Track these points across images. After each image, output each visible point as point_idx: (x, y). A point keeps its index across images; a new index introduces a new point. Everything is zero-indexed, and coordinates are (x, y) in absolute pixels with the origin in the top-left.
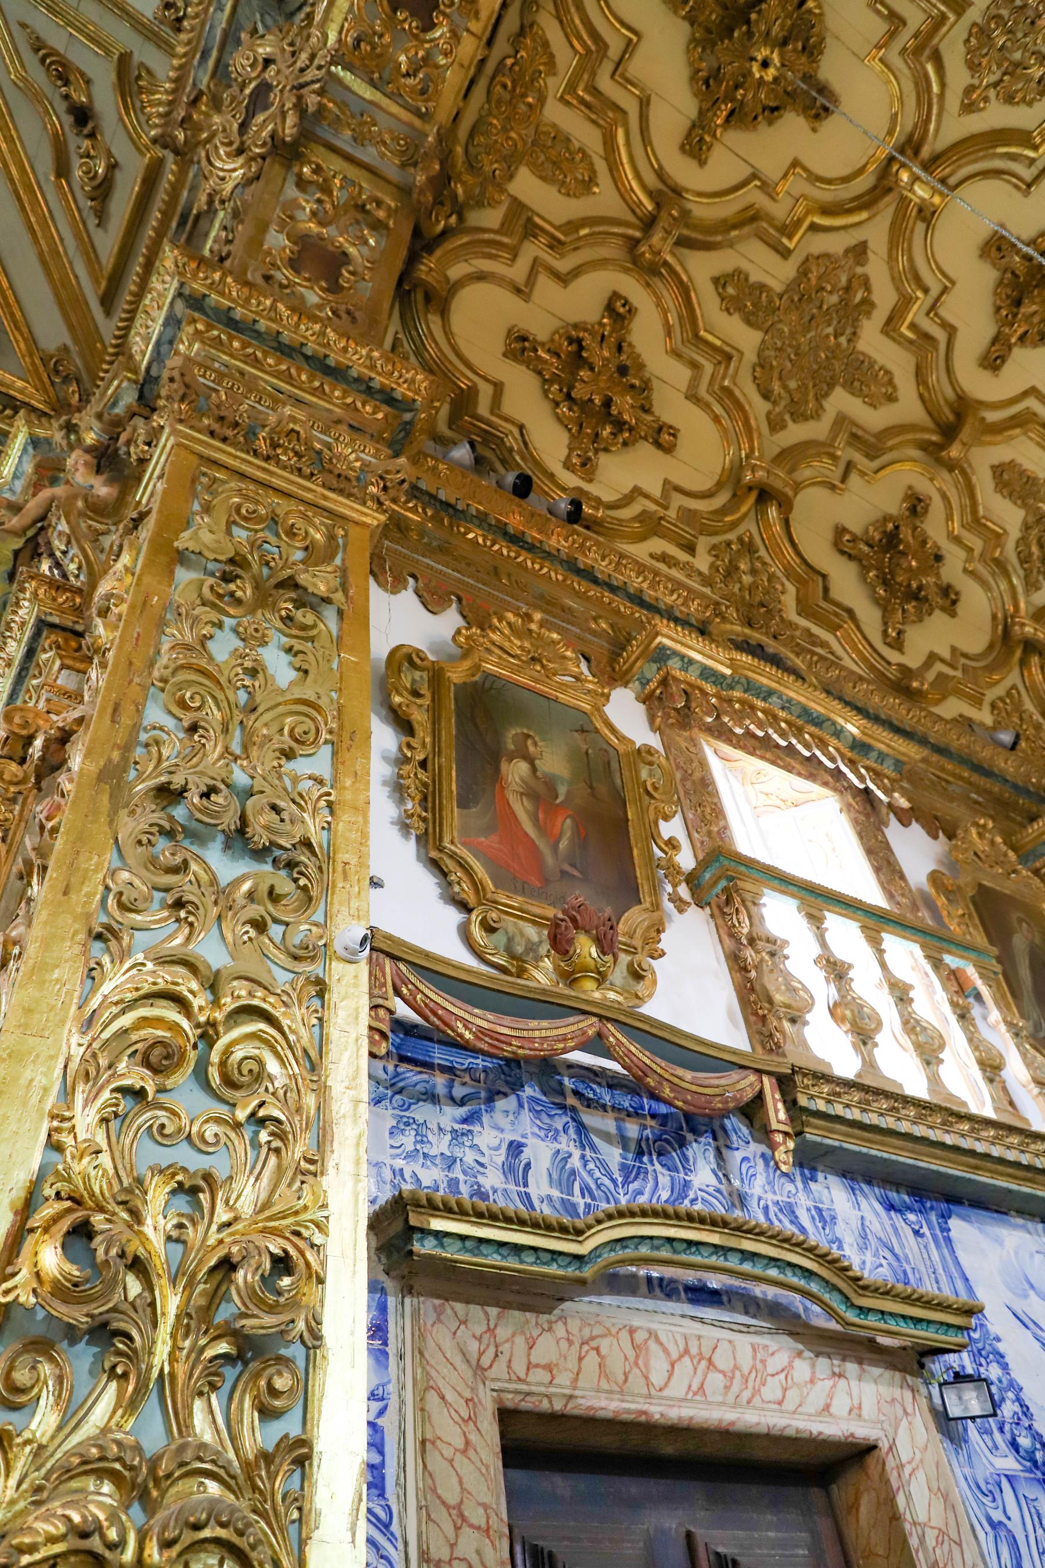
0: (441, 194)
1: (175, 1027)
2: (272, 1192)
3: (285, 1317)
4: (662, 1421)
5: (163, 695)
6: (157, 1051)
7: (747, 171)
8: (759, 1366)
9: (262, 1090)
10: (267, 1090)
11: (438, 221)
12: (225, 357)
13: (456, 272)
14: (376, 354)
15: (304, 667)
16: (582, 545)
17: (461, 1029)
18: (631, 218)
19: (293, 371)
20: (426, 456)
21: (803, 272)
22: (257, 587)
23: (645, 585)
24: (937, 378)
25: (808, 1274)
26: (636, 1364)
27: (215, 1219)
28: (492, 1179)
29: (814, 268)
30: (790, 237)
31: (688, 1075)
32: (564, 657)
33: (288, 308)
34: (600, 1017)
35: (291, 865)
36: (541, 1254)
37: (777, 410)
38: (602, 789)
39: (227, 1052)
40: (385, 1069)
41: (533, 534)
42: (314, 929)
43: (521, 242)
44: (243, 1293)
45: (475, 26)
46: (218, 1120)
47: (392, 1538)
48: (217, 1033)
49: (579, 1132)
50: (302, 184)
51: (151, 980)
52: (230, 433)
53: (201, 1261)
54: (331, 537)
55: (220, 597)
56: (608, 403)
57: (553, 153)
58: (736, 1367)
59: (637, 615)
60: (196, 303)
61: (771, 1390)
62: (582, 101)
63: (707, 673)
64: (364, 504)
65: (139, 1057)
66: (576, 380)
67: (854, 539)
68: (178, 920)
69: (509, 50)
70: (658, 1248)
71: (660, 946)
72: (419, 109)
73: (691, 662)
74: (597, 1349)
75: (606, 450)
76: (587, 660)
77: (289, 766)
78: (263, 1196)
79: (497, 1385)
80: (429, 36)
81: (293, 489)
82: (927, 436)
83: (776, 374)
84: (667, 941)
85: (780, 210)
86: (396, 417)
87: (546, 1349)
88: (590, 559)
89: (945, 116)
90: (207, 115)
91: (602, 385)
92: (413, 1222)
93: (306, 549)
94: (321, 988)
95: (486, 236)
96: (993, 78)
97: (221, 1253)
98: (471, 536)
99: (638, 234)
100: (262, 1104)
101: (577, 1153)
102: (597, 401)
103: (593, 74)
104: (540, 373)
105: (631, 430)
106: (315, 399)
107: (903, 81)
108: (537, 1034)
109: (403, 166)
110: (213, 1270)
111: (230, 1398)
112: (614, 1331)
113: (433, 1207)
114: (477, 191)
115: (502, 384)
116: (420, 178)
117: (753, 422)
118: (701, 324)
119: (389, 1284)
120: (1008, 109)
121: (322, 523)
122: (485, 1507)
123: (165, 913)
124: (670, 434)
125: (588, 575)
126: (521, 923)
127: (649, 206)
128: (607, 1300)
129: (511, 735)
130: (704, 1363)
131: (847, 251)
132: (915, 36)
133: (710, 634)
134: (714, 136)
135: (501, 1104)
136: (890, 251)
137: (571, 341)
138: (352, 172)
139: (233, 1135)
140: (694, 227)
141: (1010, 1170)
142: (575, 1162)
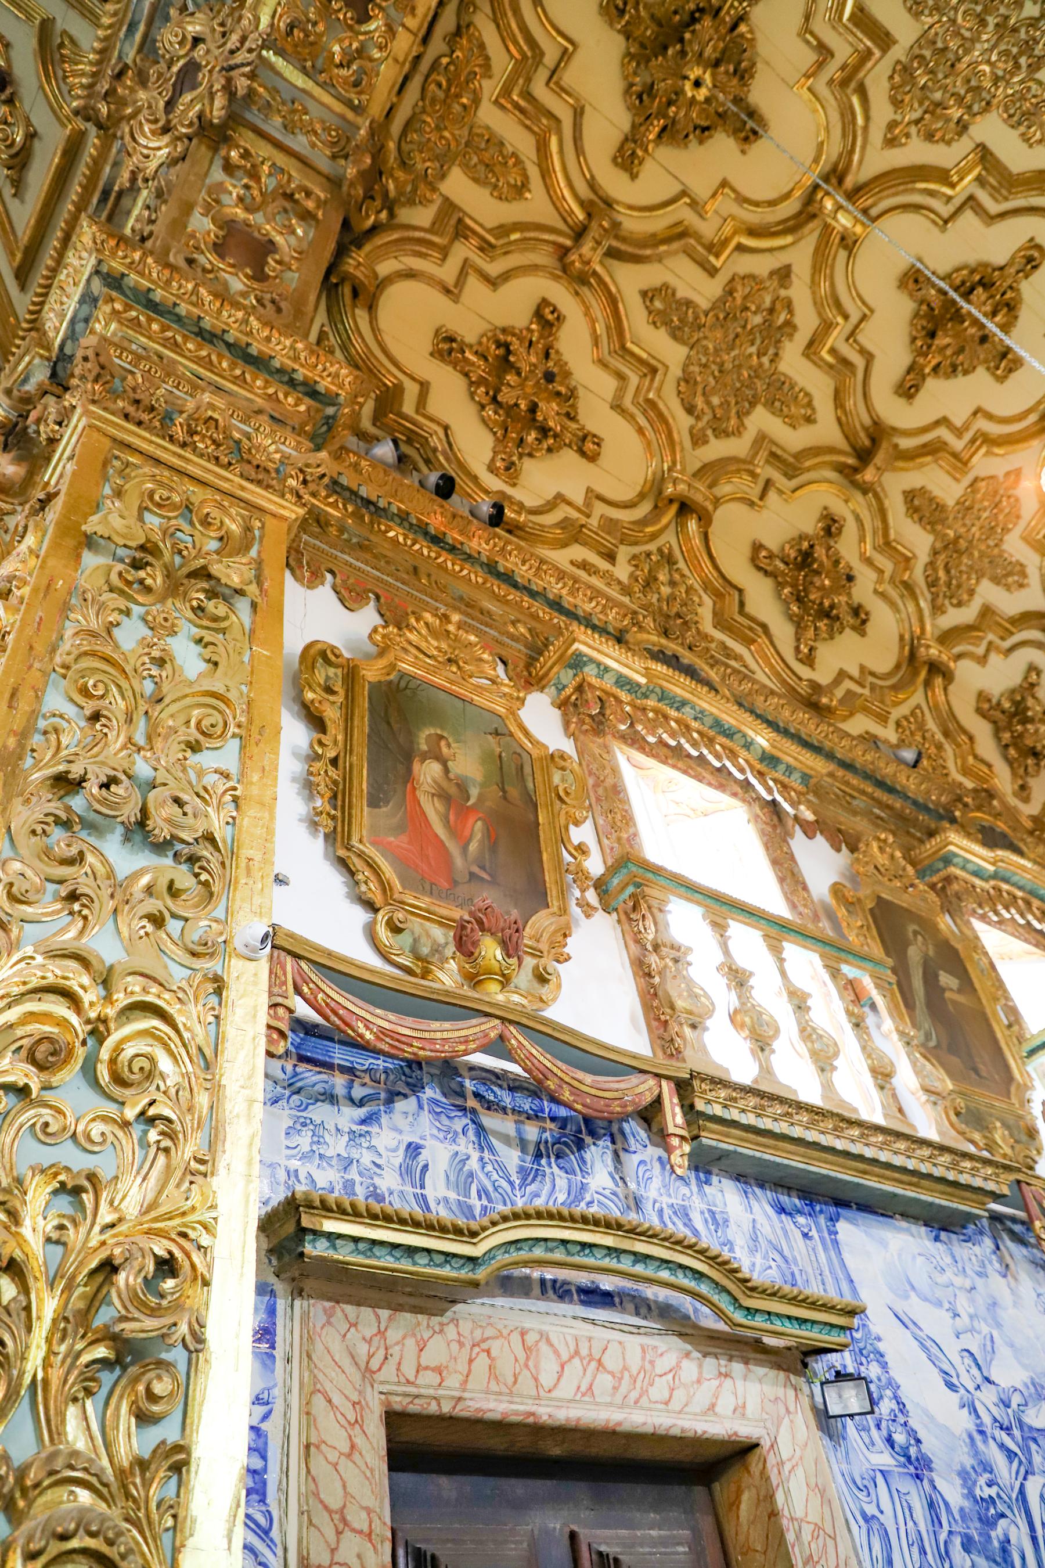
0: (372, 189)
1: (63, 1023)
2: (160, 1192)
3: (168, 1320)
4: (550, 1422)
5: (64, 682)
6: (44, 1048)
7: (677, 188)
8: (648, 1366)
9: (153, 1088)
10: (158, 1088)
11: (368, 216)
12: (143, 339)
13: (385, 268)
14: (300, 346)
15: (215, 658)
16: (503, 549)
17: (362, 1029)
18: (560, 225)
19: (214, 358)
20: (348, 451)
21: (729, 292)
22: (168, 575)
23: (564, 592)
24: (854, 402)
25: (699, 1275)
26: (526, 1366)
27: (98, 1220)
28: (389, 1181)
29: (739, 288)
30: (717, 256)
31: (588, 1079)
32: (481, 660)
33: (210, 293)
34: (502, 1019)
35: (192, 859)
36: (435, 1256)
37: (700, 425)
38: (514, 792)
39: (118, 1050)
40: (283, 1069)
41: (454, 536)
42: (214, 925)
43: (452, 242)
44: (124, 1296)
45: (412, 23)
46: (105, 1119)
47: (271, 1544)
48: (108, 1030)
49: (478, 1135)
50: (229, 168)
51: (39, 974)
52: (145, 417)
53: (81, 1263)
54: (248, 529)
55: (129, 583)
56: (533, 408)
57: (486, 156)
58: (625, 1368)
60: (114, 282)
61: (659, 1391)
62: (517, 106)
63: (622, 682)
64: (283, 496)
65: (24, 1053)
67: (771, 556)
68: (71, 913)
69: (444, 48)
70: (551, 1250)
71: (566, 950)
72: (351, 101)
73: (607, 669)
74: (488, 1352)
75: (530, 455)
76: (504, 663)
77: (194, 759)
78: (150, 1197)
79: (385, 1388)
81: (210, 478)
82: (842, 459)
84: (572, 945)
85: (707, 229)
86: (318, 411)
87: (437, 1351)
88: (510, 563)
89: (869, 147)
90: (132, 90)
91: (528, 390)
92: (305, 1223)
93: (221, 539)
94: (219, 985)
95: (418, 234)
96: (916, 115)
97: (102, 1255)
98: (391, 534)
99: (568, 243)
100: (151, 1103)
101: (475, 1155)
103: (529, 80)
104: (466, 375)
105: (556, 436)
106: (235, 388)
107: (830, 111)
108: (439, 1035)
109: (334, 157)
110: (93, 1272)
111: (107, 1404)
112: (505, 1332)
113: (326, 1208)
114: (409, 188)
116: (351, 172)
117: (676, 436)
118: (628, 336)
119: (279, 1287)
120: (928, 146)
121: (238, 514)
122: (369, 1511)
123: (58, 906)
125: (508, 579)
126: (427, 924)
127: (581, 216)
128: (500, 1301)
129: (423, 738)
130: (594, 1364)
131: (772, 273)
132: (843, 68)
133: (627, 643)
134: (646, 150)
135: (400, 1105)
137: (499, 344)
138: (281, 159)
139: (120, 1134)
140: (624, 240)
141: (897, 1175)
142: (473, 1164)
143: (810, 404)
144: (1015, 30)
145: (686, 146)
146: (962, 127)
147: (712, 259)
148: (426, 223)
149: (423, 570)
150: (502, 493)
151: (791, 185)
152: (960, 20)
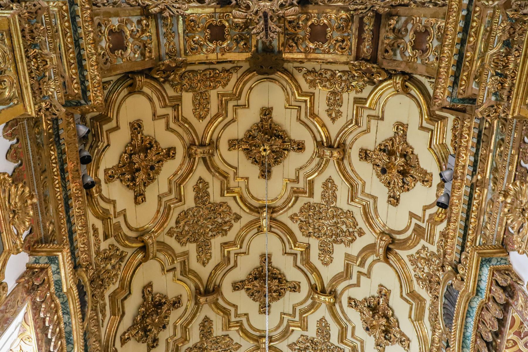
0: (167, 71)
11: (158, 75)
13: (146, 90)
16: (78, 197)
24: (220, 273)
32: (24, 223)
43: (170, 106)
56: (138, 170)
59: (65, 237)
63: (58, 283)
66: (138, 154)
69: (221, 69)
72: (186, 50)
75: (121, 181)
76: (31, 232)
80: (208, 42)
83: (186, 220)
88: (75, 204)
89: (286, 213)
95: (164, 94)
96: (303, 220)
102: (136, 166)
104: (132, 139)
107: (286, 193)
109: (167, 54)
114: (176, 83)
115: (120, 128)
116: (167, 62)
120: (298, 229)
124: (142, 199)
125: (68, 208)
132: (298, 188)
136: (244, 227)
140: (211, 160)
143: (208, 260)
144: (338, 228)
145: (248, 159)
146: (309, 235)
147: (226, 192)
148: (170, 95)
149: (46, 174)
150: (100, 181)
151: (261, 199)
152: (329, 211)
